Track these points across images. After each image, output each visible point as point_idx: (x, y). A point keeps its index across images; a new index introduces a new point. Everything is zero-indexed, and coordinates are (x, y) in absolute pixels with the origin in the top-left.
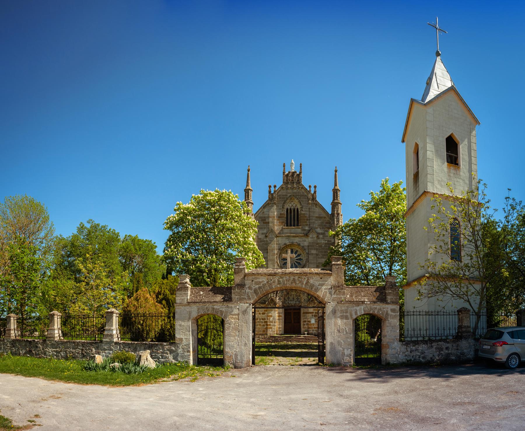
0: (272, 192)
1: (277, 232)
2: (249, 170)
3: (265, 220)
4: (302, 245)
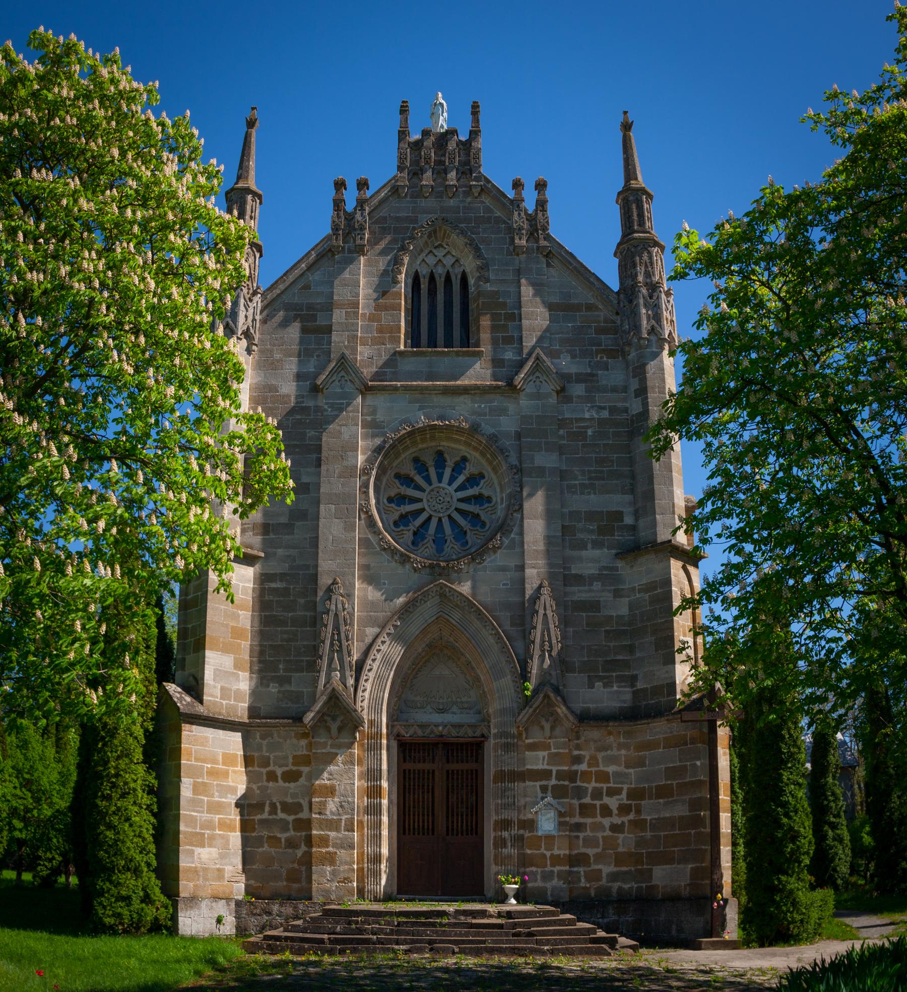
0: (350, 206)
1: (367, 372)
2: (251, 124)
4: (488, 430)
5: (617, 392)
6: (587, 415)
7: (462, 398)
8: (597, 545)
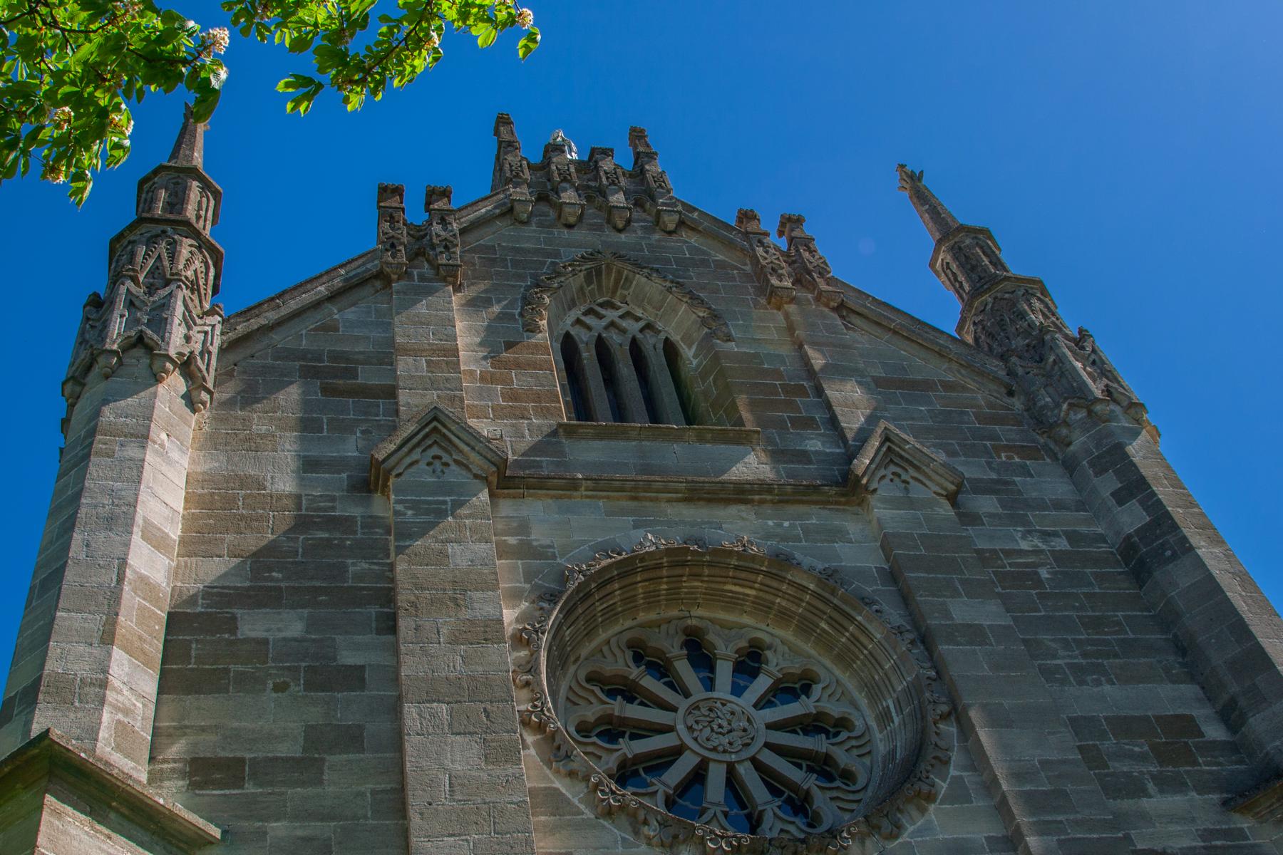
3: (352, 373)
5: (1068, 509)
6: (1024, 545)
7: (733, 510)
8: (1167, 784)
